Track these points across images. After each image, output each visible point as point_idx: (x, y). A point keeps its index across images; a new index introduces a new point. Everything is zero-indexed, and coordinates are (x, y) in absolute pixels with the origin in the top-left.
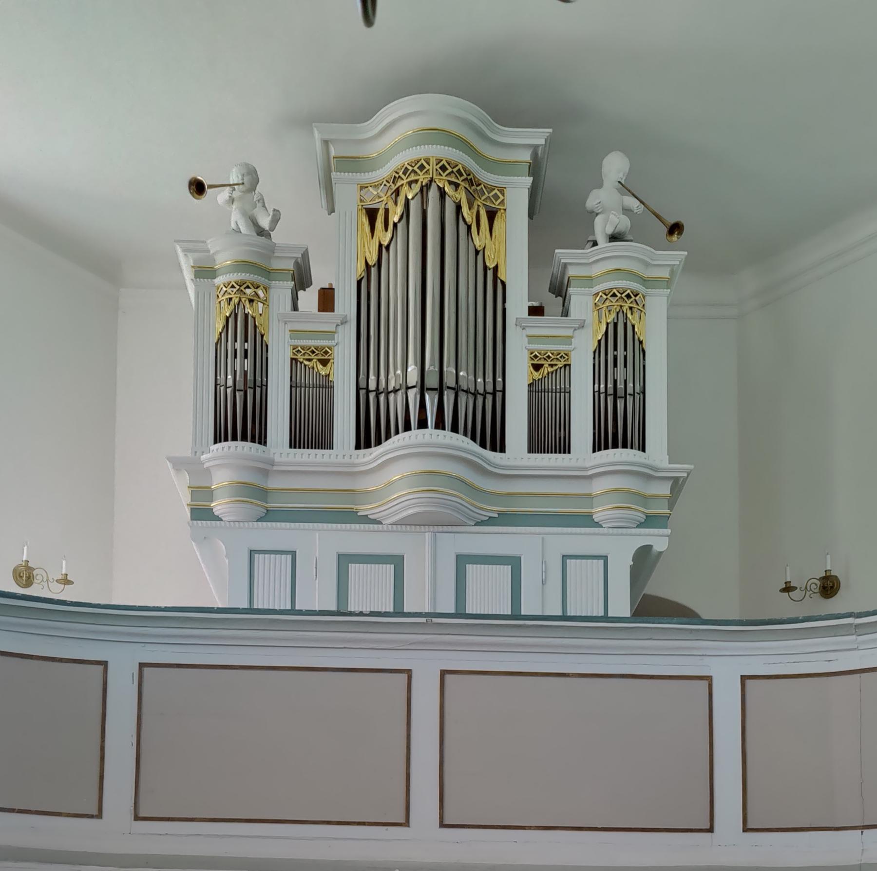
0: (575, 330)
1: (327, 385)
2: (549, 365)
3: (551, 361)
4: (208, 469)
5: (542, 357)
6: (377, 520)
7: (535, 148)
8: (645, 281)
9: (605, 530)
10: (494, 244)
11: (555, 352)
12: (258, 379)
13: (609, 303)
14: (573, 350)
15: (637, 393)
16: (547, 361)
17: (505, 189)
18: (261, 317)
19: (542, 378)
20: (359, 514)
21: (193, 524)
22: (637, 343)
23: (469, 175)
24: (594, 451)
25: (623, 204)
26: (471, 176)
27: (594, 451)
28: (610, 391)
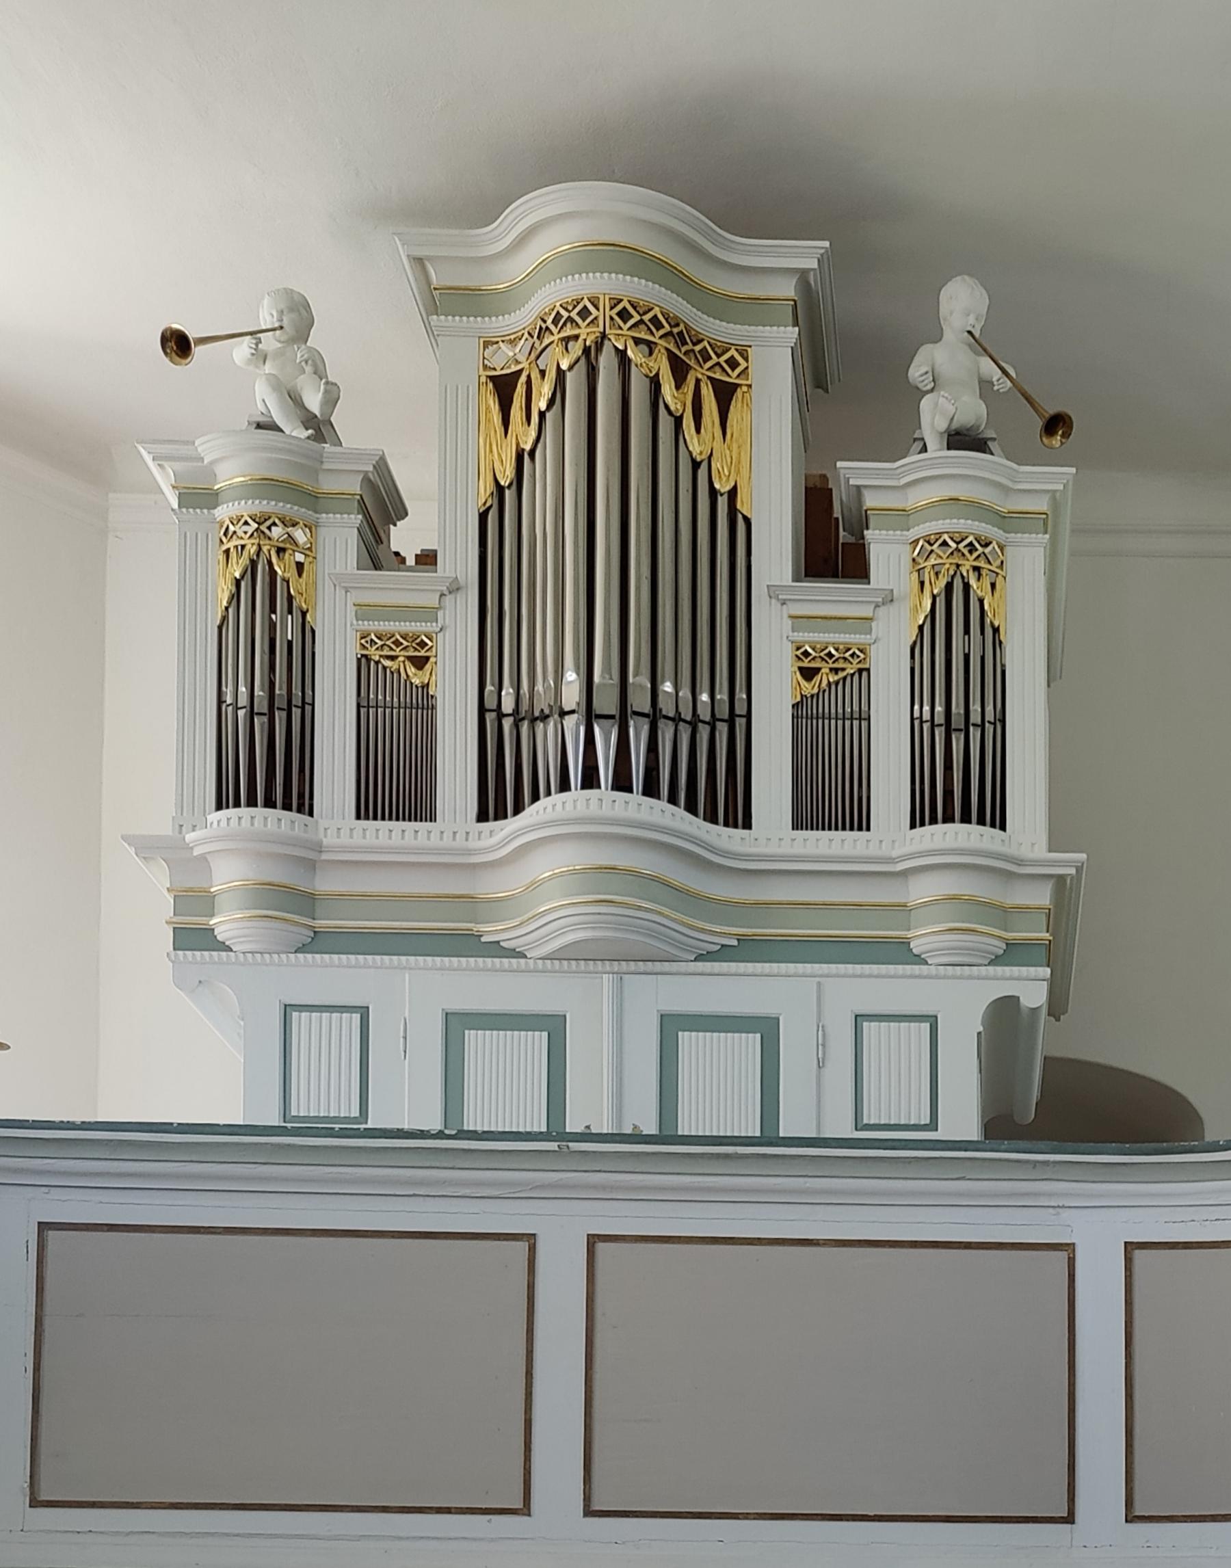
0: (877, 606)
1: (424, 702)
2: (831, 669)
3: (834, 662)
4: (203, 858)
5: (817, 655)
6: (517, 950)
7: (803, 274)
8: (1005, 520)
9: (933, 970)
10: (729, 449)
11: (841, 647)
12: (297, 692)
13: (935, 559)
14: (874, 643)
15: (989, 722)
16: (827, 662)
17: (749, 349)
18: (301, 580)
19: (818, 694)
20: (483, 939)
21: (176, 955)
22: (989, 632)
23: (677, 325)
24: (913, 826)
25: (979, 374)
26: (682, 326)
27: (913, 826)
28: (940, 718)
